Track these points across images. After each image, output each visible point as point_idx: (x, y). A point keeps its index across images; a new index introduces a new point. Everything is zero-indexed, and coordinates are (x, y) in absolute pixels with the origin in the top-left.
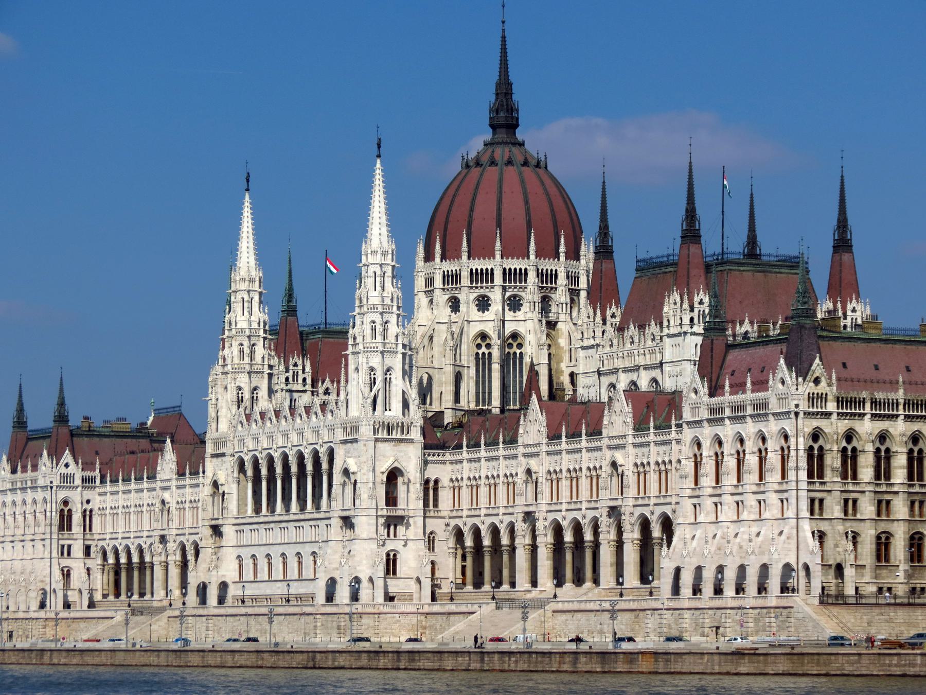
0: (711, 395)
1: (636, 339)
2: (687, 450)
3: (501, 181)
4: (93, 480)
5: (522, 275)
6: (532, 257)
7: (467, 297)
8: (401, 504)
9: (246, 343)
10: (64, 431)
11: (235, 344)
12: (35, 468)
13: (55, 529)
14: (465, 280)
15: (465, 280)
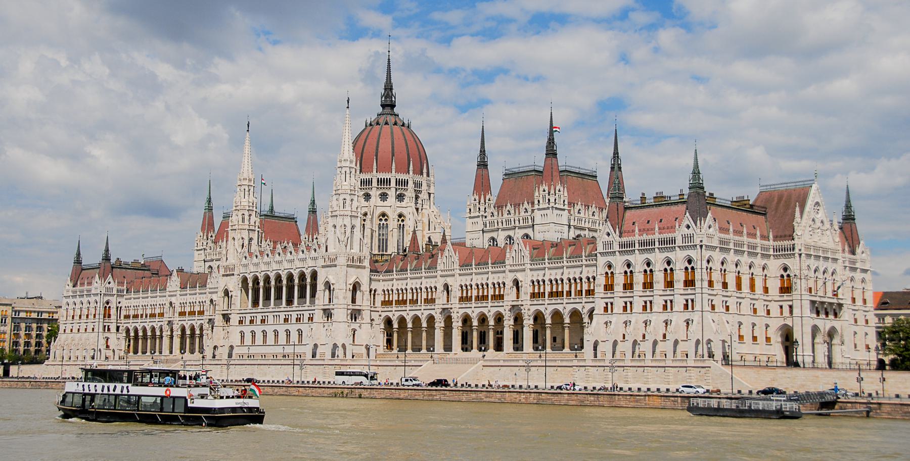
0: (620, 237)
1: (512, 212)
2: (602, 270)
3: (392, 133)
4: (123, 291)
5: (406, 183)
6: (411, 173)
7: (375, 193)
8: (358, 302)
9: (247, 213)
10: (107, 264)
11: (240, 213)
12: (90, 284)
13: (102, 317)
14: (375, 183)
15: (375, 183)
